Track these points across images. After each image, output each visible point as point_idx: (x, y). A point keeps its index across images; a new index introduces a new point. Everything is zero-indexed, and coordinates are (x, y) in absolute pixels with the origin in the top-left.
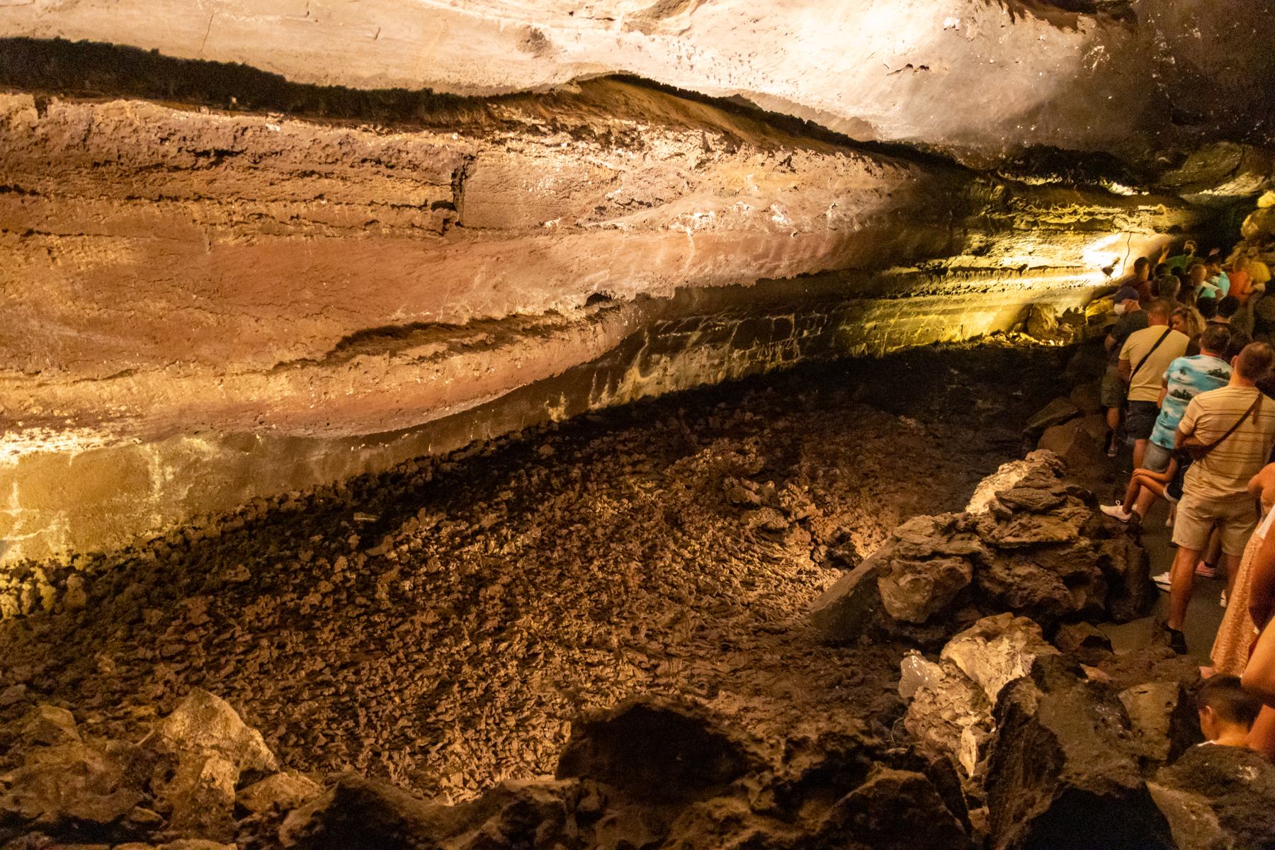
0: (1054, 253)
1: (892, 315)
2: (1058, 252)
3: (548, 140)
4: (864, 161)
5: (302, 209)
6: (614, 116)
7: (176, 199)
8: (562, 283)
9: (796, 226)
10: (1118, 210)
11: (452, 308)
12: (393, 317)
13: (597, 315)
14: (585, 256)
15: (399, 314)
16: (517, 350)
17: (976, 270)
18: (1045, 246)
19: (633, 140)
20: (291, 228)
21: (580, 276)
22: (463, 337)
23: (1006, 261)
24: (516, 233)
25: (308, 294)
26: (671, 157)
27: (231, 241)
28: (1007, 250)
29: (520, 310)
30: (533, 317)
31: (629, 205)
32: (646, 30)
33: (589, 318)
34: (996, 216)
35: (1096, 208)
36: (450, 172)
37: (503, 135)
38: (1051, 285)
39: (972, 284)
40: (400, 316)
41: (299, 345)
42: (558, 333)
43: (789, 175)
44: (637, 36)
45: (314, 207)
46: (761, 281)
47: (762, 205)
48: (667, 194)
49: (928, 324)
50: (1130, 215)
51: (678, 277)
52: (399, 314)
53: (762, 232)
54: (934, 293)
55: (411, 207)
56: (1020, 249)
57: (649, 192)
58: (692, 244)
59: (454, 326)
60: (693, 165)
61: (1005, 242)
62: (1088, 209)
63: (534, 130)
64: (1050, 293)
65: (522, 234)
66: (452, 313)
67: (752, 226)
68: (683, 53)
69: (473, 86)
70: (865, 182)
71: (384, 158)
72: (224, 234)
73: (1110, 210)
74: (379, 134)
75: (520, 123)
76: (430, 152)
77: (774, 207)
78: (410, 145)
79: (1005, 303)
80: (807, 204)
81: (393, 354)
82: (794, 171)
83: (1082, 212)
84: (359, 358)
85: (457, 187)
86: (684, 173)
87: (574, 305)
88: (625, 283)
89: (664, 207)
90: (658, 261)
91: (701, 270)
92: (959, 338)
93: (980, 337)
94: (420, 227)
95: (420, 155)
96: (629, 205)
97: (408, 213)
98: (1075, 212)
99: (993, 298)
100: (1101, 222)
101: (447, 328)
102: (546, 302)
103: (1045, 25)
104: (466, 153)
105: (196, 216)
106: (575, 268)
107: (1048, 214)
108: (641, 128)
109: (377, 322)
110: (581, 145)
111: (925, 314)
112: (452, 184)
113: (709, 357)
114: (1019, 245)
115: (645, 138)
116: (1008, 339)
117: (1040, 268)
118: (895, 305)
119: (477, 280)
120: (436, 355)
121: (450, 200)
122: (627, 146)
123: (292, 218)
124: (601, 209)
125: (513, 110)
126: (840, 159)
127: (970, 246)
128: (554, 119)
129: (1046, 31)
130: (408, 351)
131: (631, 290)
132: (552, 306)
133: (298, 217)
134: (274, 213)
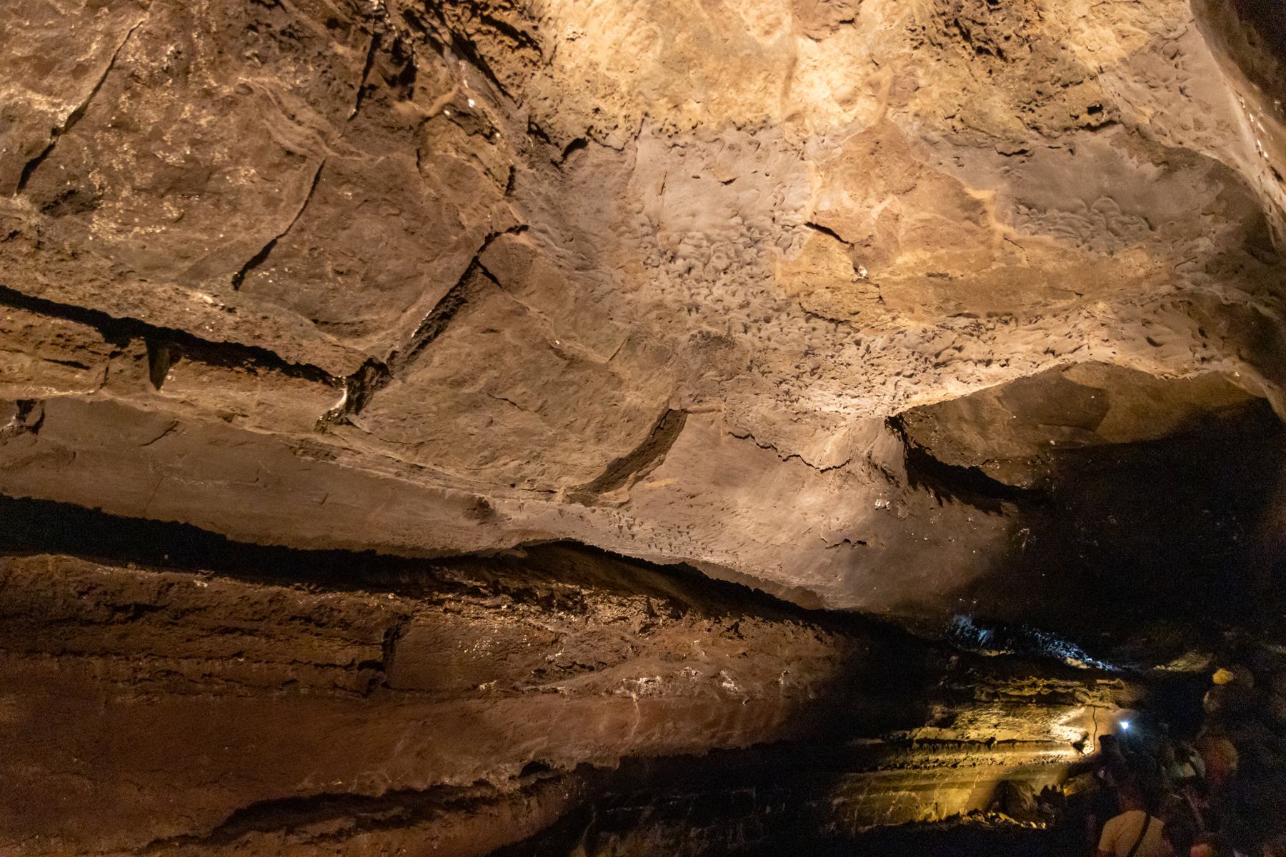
0: (1021, 726)
1: (860, 790)
2: (1024, 728)
3: (488, 602)
4: (813, 628)
5: (217, 666)
6: (559, 580)
7: (80, 654)
8: (496, 751)
9: (747, 693)
10: (1077, 683)
11: (369, 776)
12: (299, 787)
13: (533, 786)
14: (521, 720)
15: (307, 783)
16: (435, 827)
17: (944, 742)
18: (1010, 719)
19: (576, 603)
20: (200, 686)
21: (514, 743)
22: (374, 811)
23: (973, 734)
24: (446, 695)
25: (205, 760)
26: (615, 621)
27: (130, 700)
28: (971, 722)
29: (447, 781)
30: (460, 788)
31: (570, 669)
32: (587, 503)
33: (526, 791)
34: (955, 687)
35: (1053, 681)
36: (383, 632)
37: (442, 596)
39: (940, 758)
40: (308, 785)
41: (183, 819)
42: (486, 808)
43: (736, 642)
44: (578, 507)
45: (230, 665)
46: (714, 751)
47: (711, 670)
48: (610, 658)
49: (900, 801)
50: (1091, 690)
51: (623, 745)
52: (307, 783)
53: (713, 698)
54: (902, 767)
55: (335, 666)
56: (985, 722)
57: (591, 656)
58: (637, 710)
59: (367, 798)
60: (637, 629)
61: (968, 714)
63: (475, 592)
64: (1022, 769)
65: (452, 698)
66: (368, 782)
67: (702, 693)
68: (623, 523)
69: (414, 549)
70: (817, 650)
71: (315, 616)
72: (124, 692)
73: (1069, 683)
74: (312, 592)
75: (461, 584)
76: (363, 611)
77: (723, 672)
78: (344, 603)
79: (978, 779)
80: (758, 670)
81: (290, 831)
82: (741, 637)
83: (1042, 685)
84: (249, 836)
85: (388, 647)
86: (628, 637)
87: (507, 775)
88: (565, 751)
89: (607, 671)
90: (601, 728)
91: (649, 738)
92: (934, 817)
93: (957, 816)
94: (344, 688)
95: (353, 613)
96: (570, 669)
97: (330, 673)
98: (1034, 685)
99: (962, 774)
100: (1063, 695)
101: (359, 800)
102: (476, 770)
103: (971, 509)
104: (401, 613)
105: (98, 672)
106: (509, 734)
107: (1007, 686)
108: (584, 592)
109: (279, 792)
110: (522, 607)
111: (896, 789)
112: (384, 644)
113: (663, 837)
115: (588, 601)
116: (987, 819)
117: (1008, 741)
118: (859, 780)
119: (400, 746)
120: (340, 832)
121: (380, 660)
122: (570, 609)
123: (204, 675)
124: (540, 672)
125: (455, 572)
126: (789, 627)
127: (932, 717)
128: (497, 582)
129: (973, 515)
130: (309, 828)
131: (571, 759)
132: (483, 776)
133: (210, 675)
134: (186, 670)
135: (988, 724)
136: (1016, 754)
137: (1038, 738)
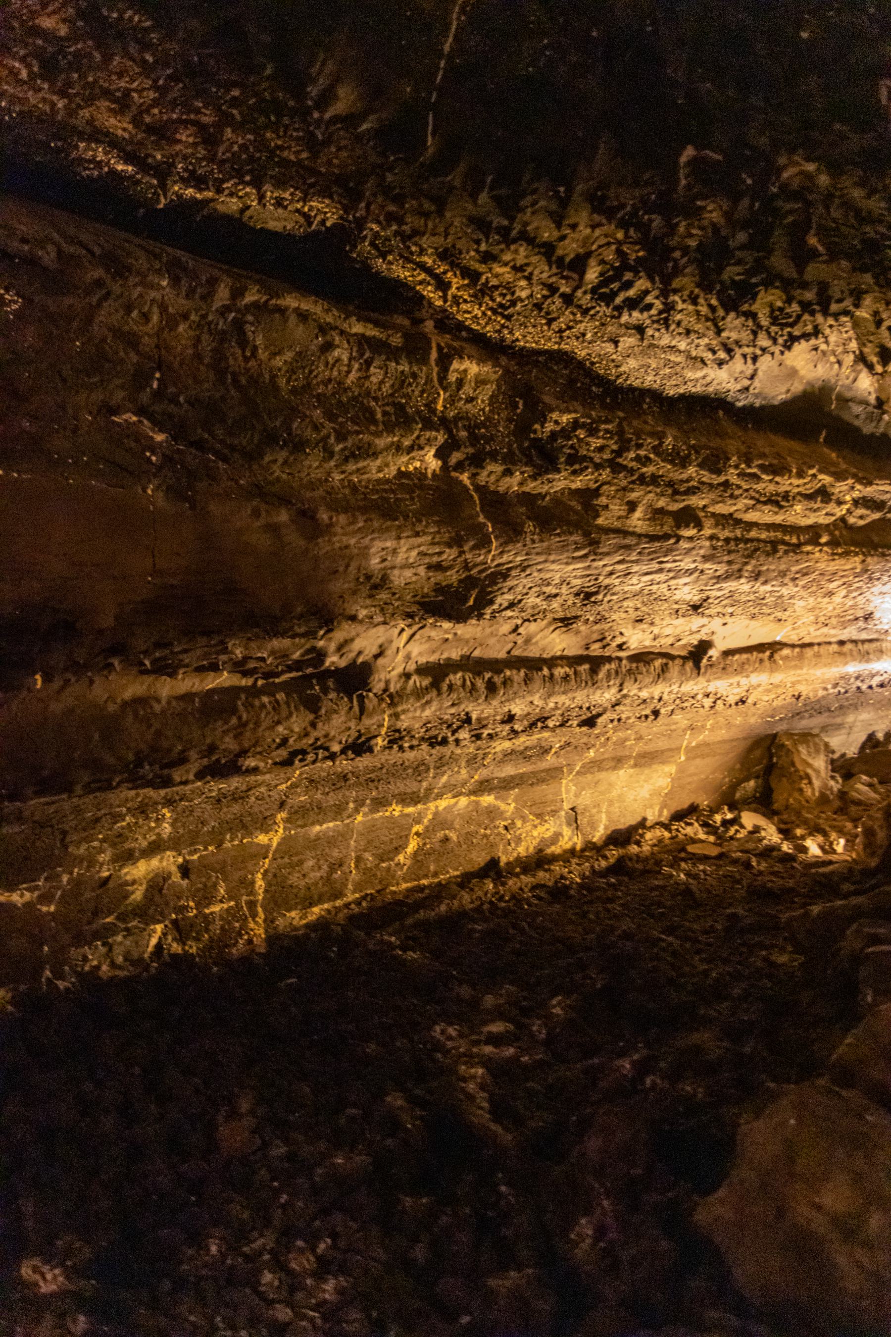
18: (743, 586)
38: (804, 689)
49: (440, 822)
62: (861, 490)
79: (689, 740)
92: (570, 839)
98: (824, 494)
114: (635, 583)
117: (760, 648)
135: (662, 598)
136: (777, 678)
137: (845, 635)
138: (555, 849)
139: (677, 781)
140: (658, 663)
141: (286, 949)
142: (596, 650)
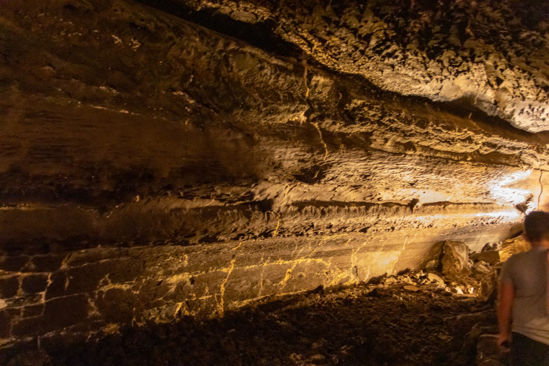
2: (459, 186)
10: (523, 144)
18: (433, 176)
35: (495, 139)
38: (459, 223)
49: (299, 268)
62: (486, 139)
64: (458, 230)
73: (515, 143)
79: (407, 241)
83: (480, 141)
92: (353, 280)
100: (507, 157)
114: (386, 173)
117: (439, 203)
135: (396, 180)
136: (447, 216)
137: (477, 200)
138: (347, 284)
139: (401, 259)
140: (395, 207)
141: (233, 318)
142: (368, 200)
